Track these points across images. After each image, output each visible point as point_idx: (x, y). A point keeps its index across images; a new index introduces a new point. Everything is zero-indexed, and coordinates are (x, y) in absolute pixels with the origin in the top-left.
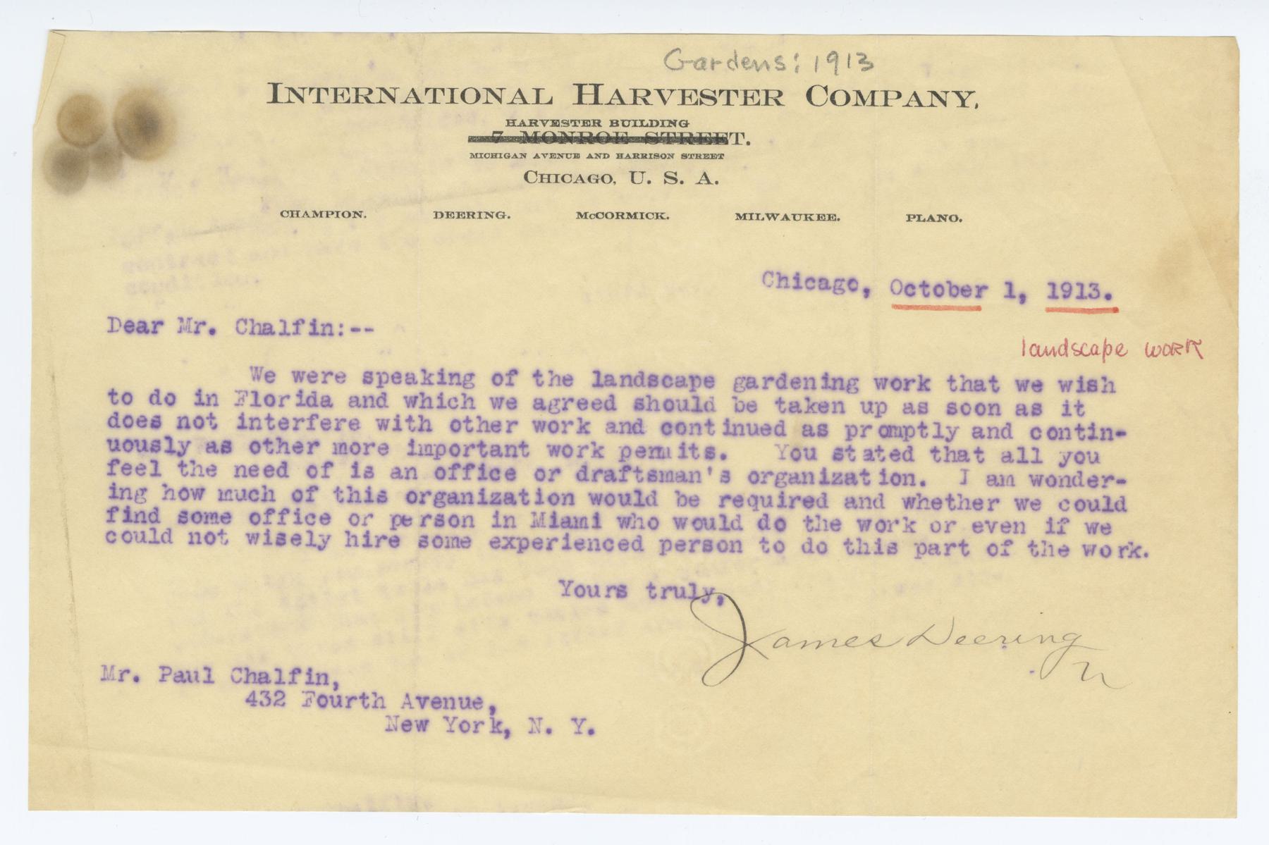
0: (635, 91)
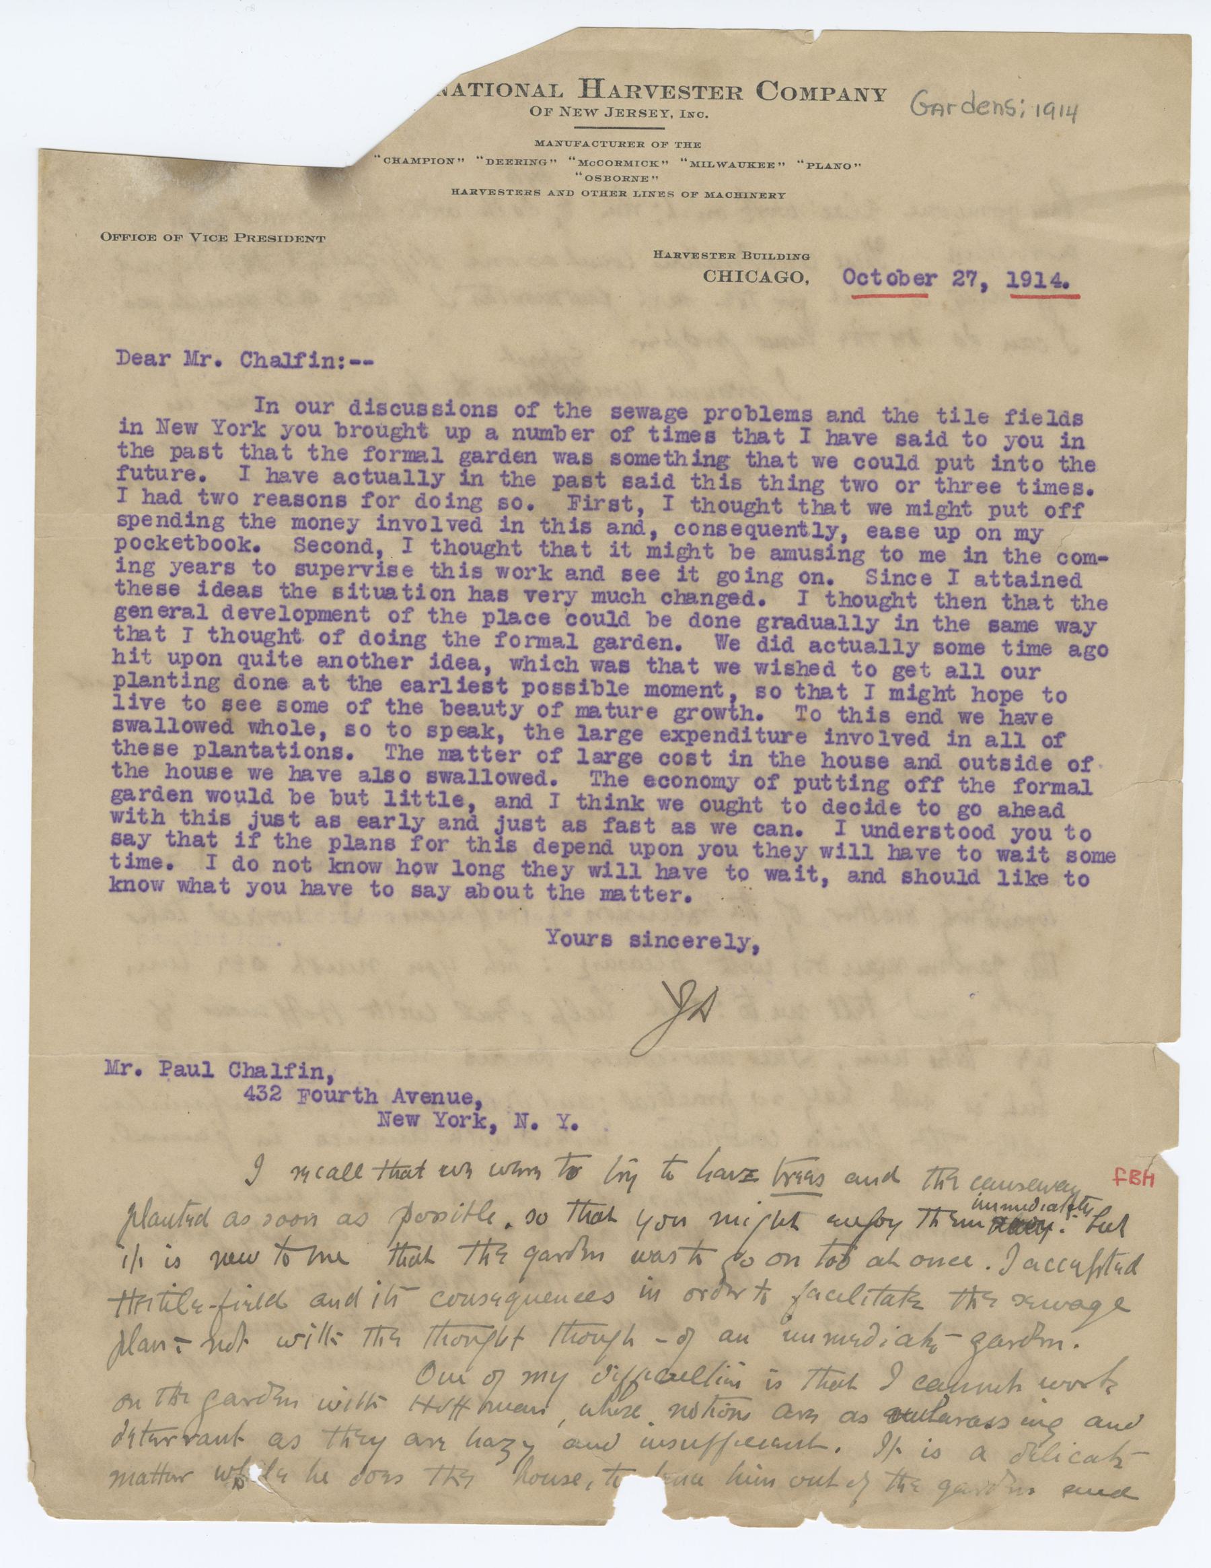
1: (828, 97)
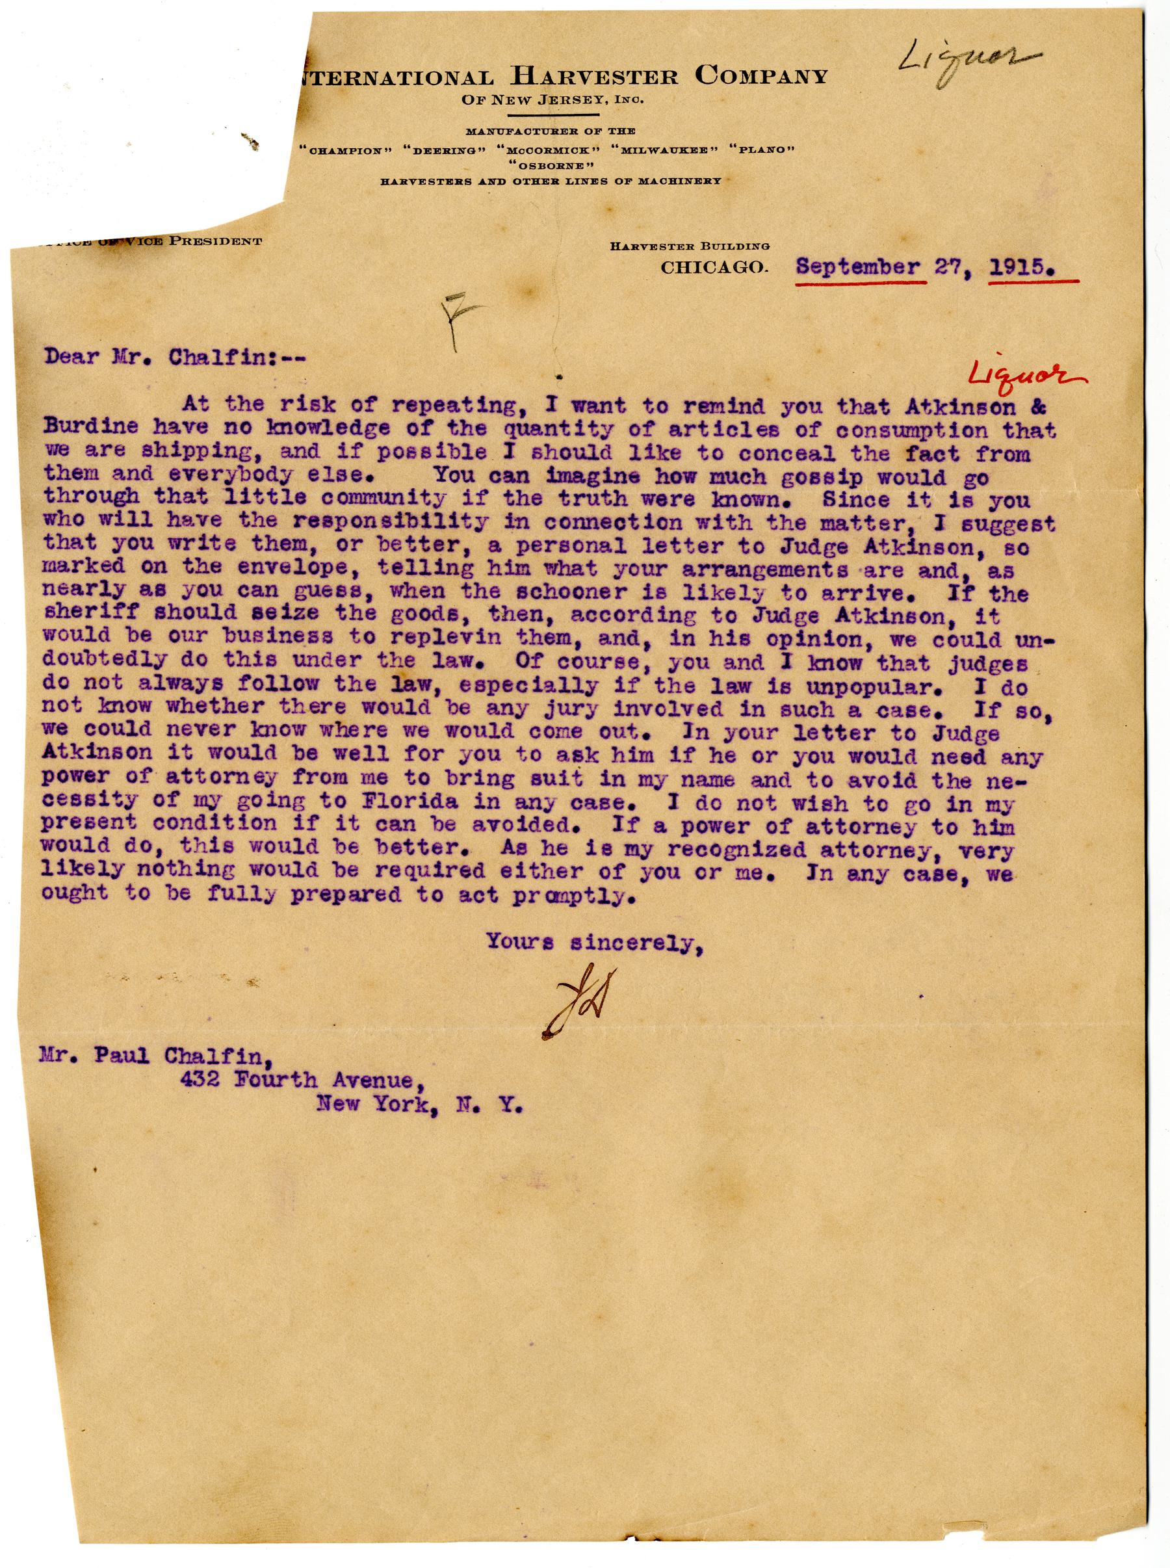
0: (562, 73)
1: (768, 80)
